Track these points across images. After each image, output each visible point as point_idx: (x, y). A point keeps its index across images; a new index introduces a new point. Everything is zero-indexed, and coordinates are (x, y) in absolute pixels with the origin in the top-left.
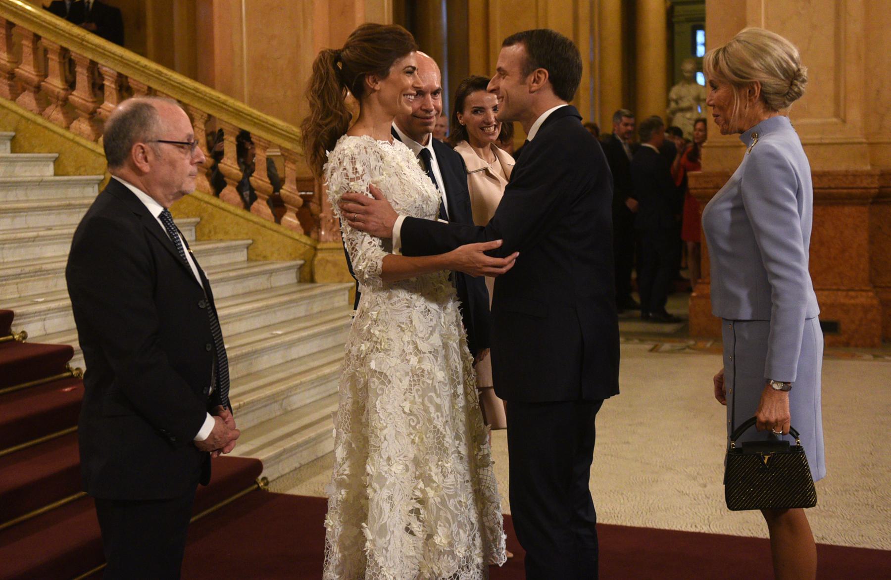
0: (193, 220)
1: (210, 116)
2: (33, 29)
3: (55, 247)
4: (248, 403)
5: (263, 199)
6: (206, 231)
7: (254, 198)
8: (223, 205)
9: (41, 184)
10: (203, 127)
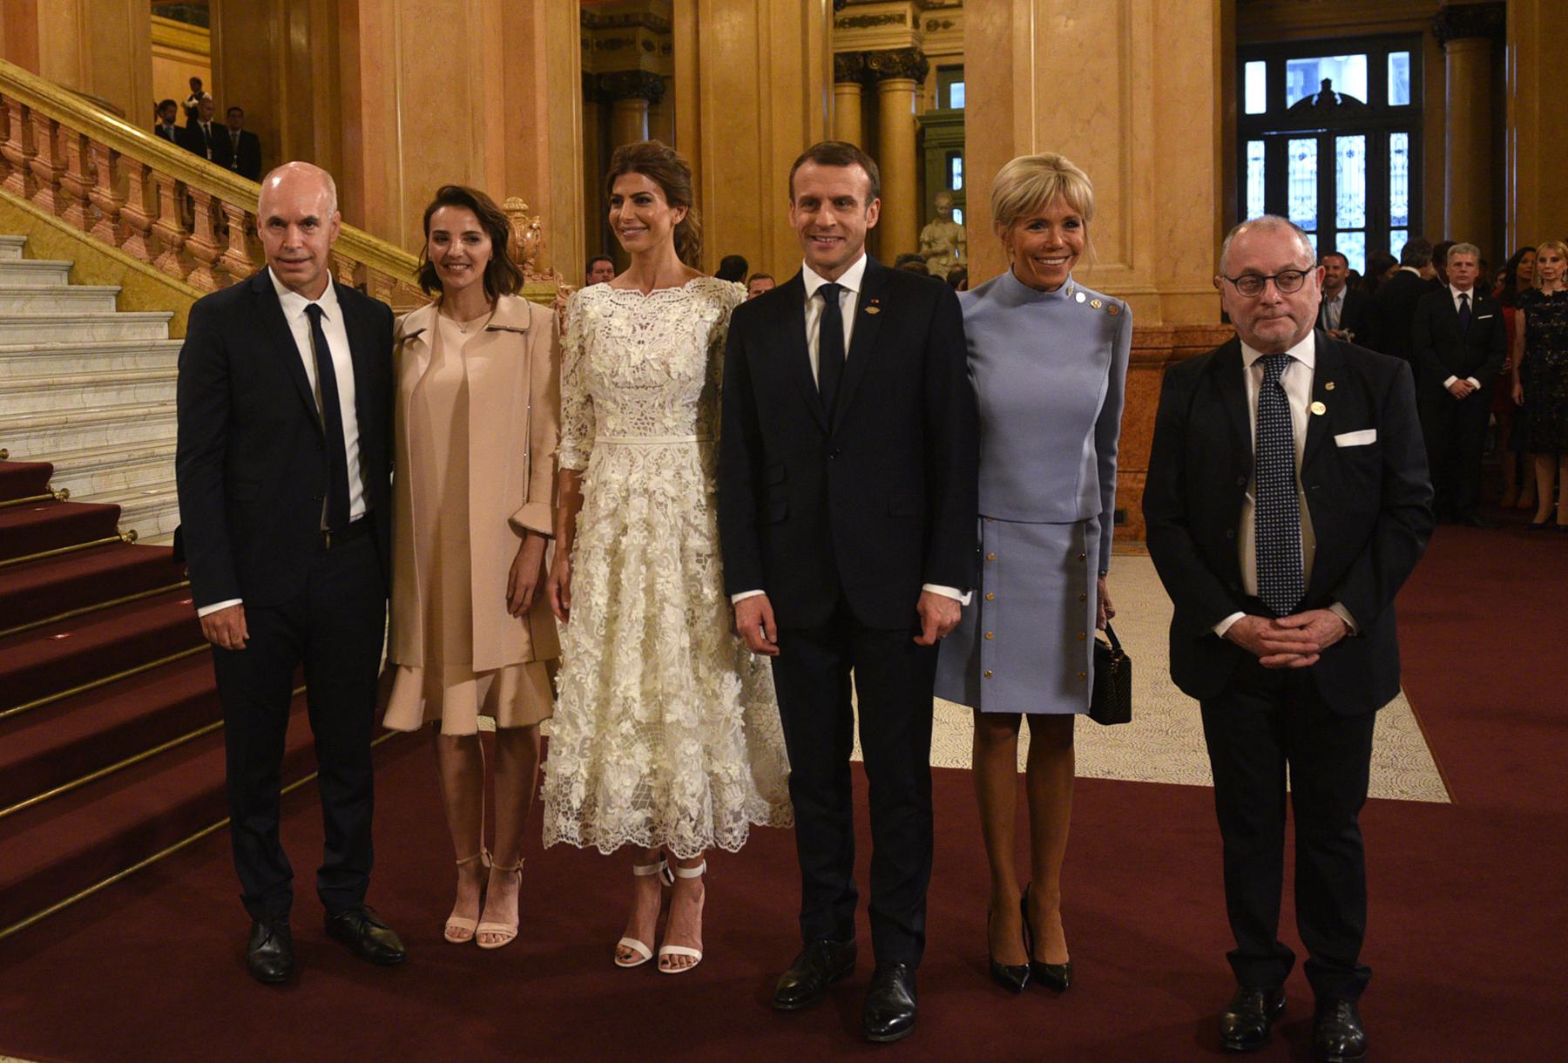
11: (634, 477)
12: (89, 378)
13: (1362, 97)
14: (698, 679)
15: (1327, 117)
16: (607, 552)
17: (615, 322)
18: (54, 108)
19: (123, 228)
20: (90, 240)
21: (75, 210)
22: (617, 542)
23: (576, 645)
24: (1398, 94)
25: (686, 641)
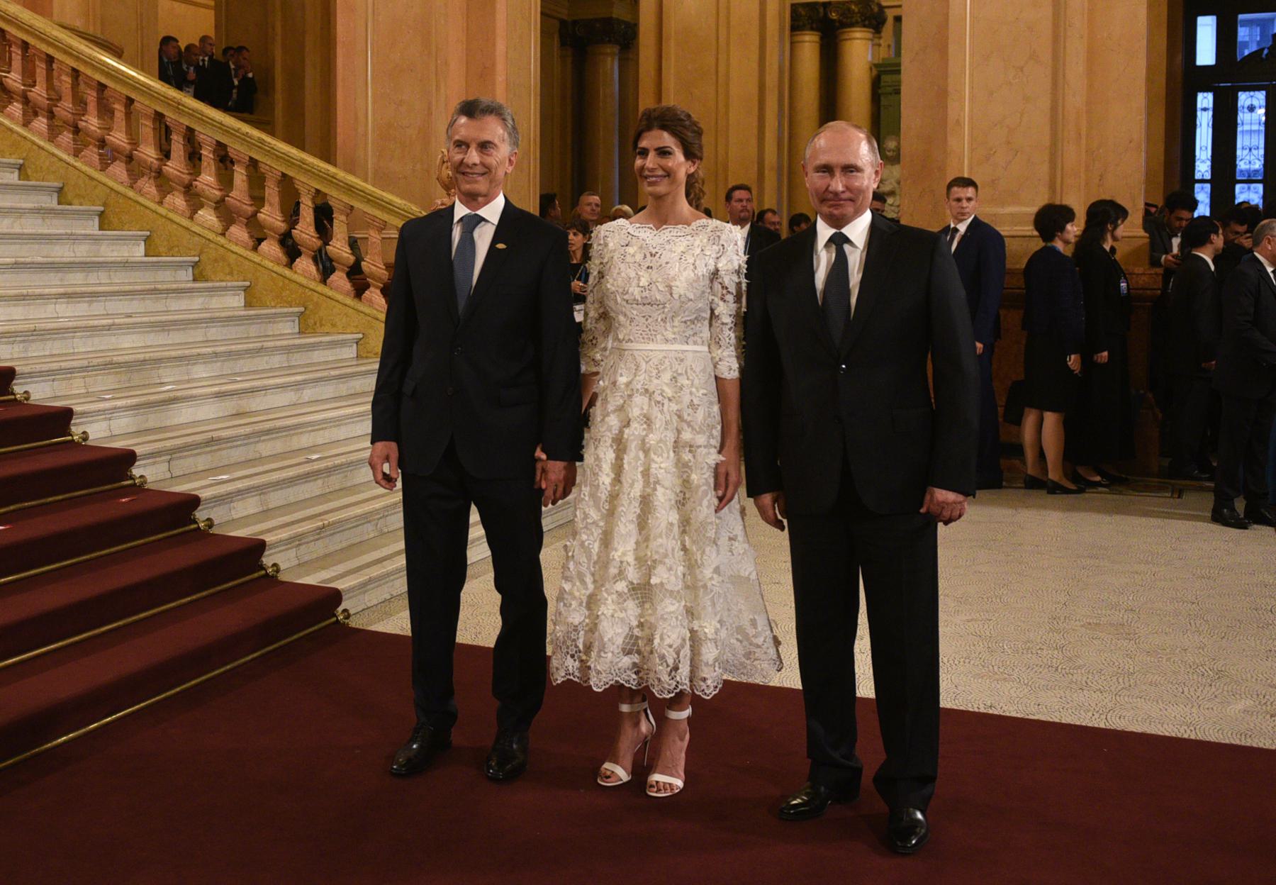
0: (296, 309)
1: (318, 191)
2: (126, 91)
3: (134, 337)
4: (334, 523)
5: (377, 287)
6: (311, 322)
7: (367, 286)
8: (330, 293)
9: (126, 265)
10: (310, 204)
12: (62, 290)
14: (684, 549)
16: (614, 440)
20: (78, 164)
21: (66, 137)
22: (621, 432)
23: (586, 516)
25: (674, 517)
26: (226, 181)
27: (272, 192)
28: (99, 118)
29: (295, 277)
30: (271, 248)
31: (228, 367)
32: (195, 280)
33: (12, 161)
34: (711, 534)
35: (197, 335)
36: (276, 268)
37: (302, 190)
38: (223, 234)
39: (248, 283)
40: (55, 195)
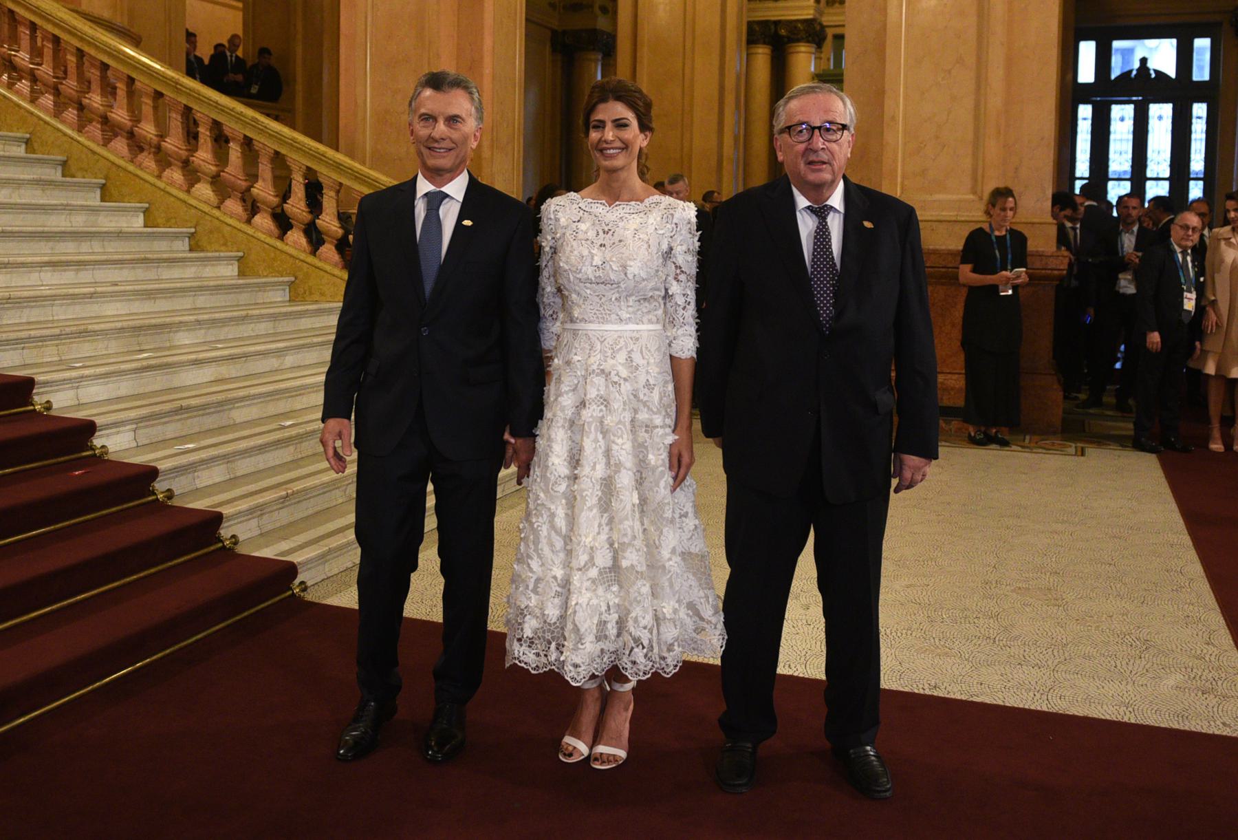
0: (286, 279)
3: (119, 305)
4: (298, 492)
6: (301, 290)
8: (320, 264)
9: (120, 235)
10: (301, 180)
11: (592, 360)
13: (1172, 73)
15: (1143, 87)
17: (583, 226)
18: (56, 25)
19: (110, 129)
20: (81, 139)
21: (71, 114)
23: (537, 498)
24: (1201, 71)
26: (221, 157)
27: (265, 169)
28: (102, 95)
29: (286, 248)
30: (263, 221)
31: (213, 334)
32: (191, 250)
33: (19, 135)
34: (668, 514)
35: (186, 303)
36: (269, 240)
37: (294, 167)
38: (218, 208)
39: (241, 254)
40: (59, 169)
